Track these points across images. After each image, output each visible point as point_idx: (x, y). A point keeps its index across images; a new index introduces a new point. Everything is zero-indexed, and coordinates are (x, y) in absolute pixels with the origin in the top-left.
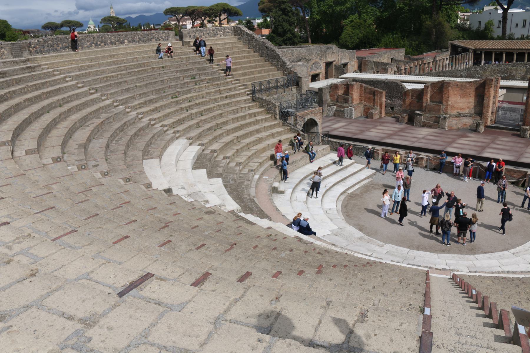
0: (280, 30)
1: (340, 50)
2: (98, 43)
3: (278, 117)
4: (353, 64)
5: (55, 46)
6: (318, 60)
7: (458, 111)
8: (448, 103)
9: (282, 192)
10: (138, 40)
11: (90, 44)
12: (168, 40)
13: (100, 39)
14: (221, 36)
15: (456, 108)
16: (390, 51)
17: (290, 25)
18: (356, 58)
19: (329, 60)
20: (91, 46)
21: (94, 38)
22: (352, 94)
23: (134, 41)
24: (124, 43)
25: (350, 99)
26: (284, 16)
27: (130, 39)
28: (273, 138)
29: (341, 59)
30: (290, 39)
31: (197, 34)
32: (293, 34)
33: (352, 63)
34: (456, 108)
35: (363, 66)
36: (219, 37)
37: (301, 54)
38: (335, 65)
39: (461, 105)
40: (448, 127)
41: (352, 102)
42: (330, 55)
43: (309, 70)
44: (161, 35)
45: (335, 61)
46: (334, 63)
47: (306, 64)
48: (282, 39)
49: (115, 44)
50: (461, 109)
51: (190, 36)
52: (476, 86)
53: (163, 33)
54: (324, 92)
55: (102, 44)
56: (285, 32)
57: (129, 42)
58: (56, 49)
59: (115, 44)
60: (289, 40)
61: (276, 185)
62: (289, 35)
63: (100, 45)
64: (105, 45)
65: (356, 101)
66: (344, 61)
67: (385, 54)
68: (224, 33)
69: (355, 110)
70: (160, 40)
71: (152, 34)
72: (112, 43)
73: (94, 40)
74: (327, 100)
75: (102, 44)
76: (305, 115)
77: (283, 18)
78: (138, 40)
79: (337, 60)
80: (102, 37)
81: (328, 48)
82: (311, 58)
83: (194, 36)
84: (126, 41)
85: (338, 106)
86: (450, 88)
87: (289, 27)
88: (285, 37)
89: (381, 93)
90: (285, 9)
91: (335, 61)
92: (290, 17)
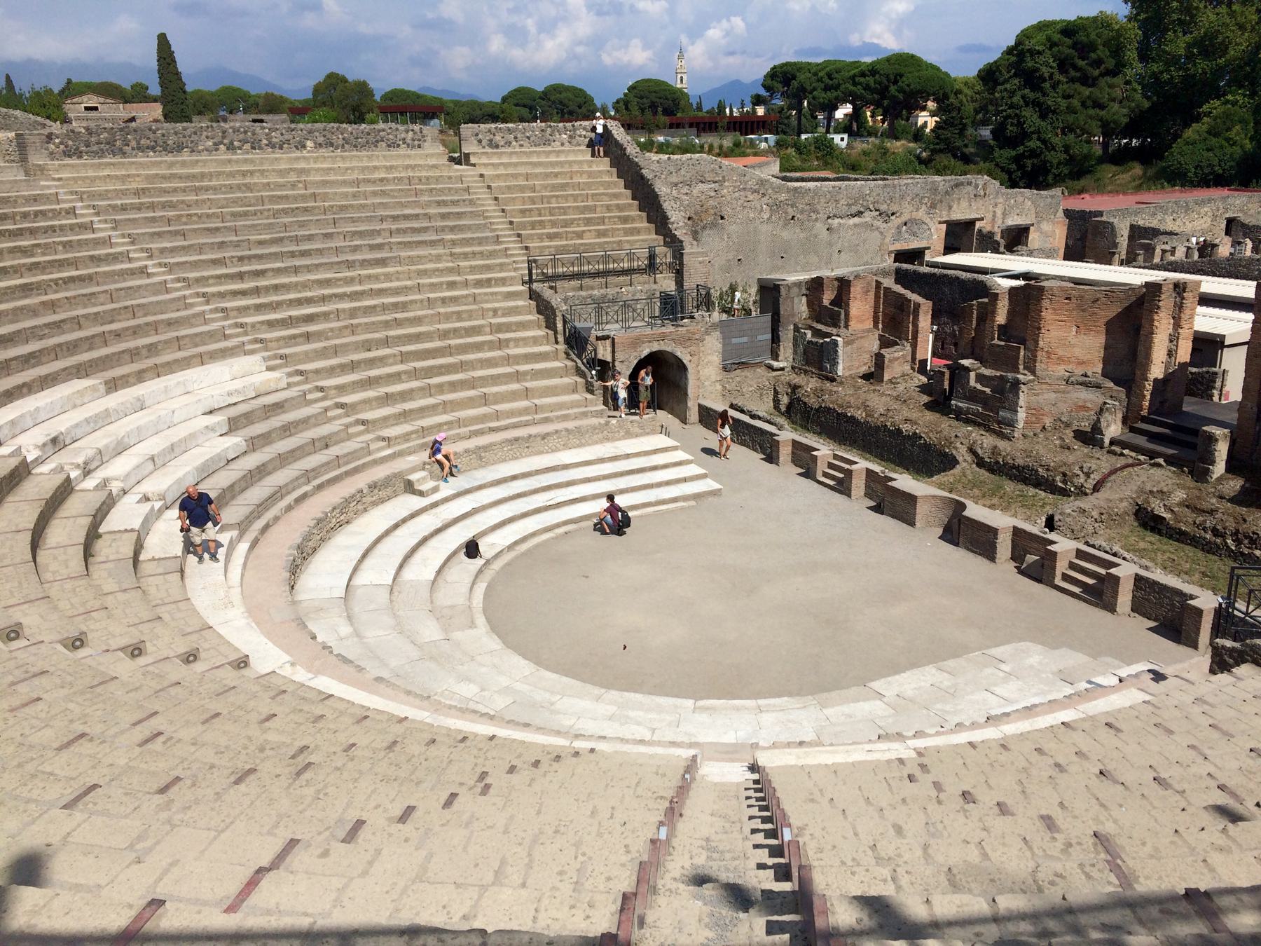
0: (1011, 129)
1: (1003, 189)
2: (236, 143)
3: (561, 338)
4: (1052, 231)
5: (118, 143)
6: (921, 214)
7: (1069, 368)
8: (1037, 342)
9: (421, 494)
10: (341, 142)
11: (215, 144)
12: (419, 146)
13: (242, 136)
14: (563, 144)
15: (1061, 360)
16: (1224, 199)
17: (1043, 116)
18: (1061, 214)
19: (961, 213)
20: (217, 150)
21: (224, 132)
22: (848, 305)
23: (332, 145)
24: (304, 147)
25: (843, 316)
26: (1027, 91)
27: (321, 139)
28: (518, 381)
29: (1004, 215)
30: (1033, 154)
31: (498, 138)
32: (1044, 142)
33: (1046, 226)
34: (1061, 360)
35: (1090, 236)
36: (556, 146)
37: (863, 197)
38: (980, 231)
39: (1078, 352)
40: (1028, 408)
41: (846, 326)
42: (964, 204)
43: (887, 240)
44: (403, 135)
45: (982, 219)
46: (978, 225)
47: (879, 223)
48: (1013, 153)
49: (281, 148)
50: (1081, 363)
51: (480, 141)
52: (1127, 303)
53: (407, 131)
54: (783, 291)
55: (247, 146)
56: (1024, 136)
57: (319, 145)
58: (121, 150)
59: (281, 148)
60: (1030, 157)
61: (413, 477)
62: (1033, 144)
63: (240, 148)
64: (253, 148)
65: (861, 321)
66: (1014, 220)
67: (1201, 203)
68: (570, 137)
69: (847, 343)
70: (399, 146)
71: (379, 131)
72: (271, 145)
73: (224, 137)
74: (793, 315)
75: (247, 146)
76: (643, 342)
77: (1023, 97)
78: (341, 142)
79: (989, 216)
80: (246, 132)
81: (957, 185)
82: (894, 208)
83: (491, 141)
84: (309, 144)
85: (817, 333)
86: (1045, 303)
87: (1038, 122)
88: (1021, 149)
89: (917, 306)
90: (1037, 70)
91: (982, 219)
92: (1045, 94)
